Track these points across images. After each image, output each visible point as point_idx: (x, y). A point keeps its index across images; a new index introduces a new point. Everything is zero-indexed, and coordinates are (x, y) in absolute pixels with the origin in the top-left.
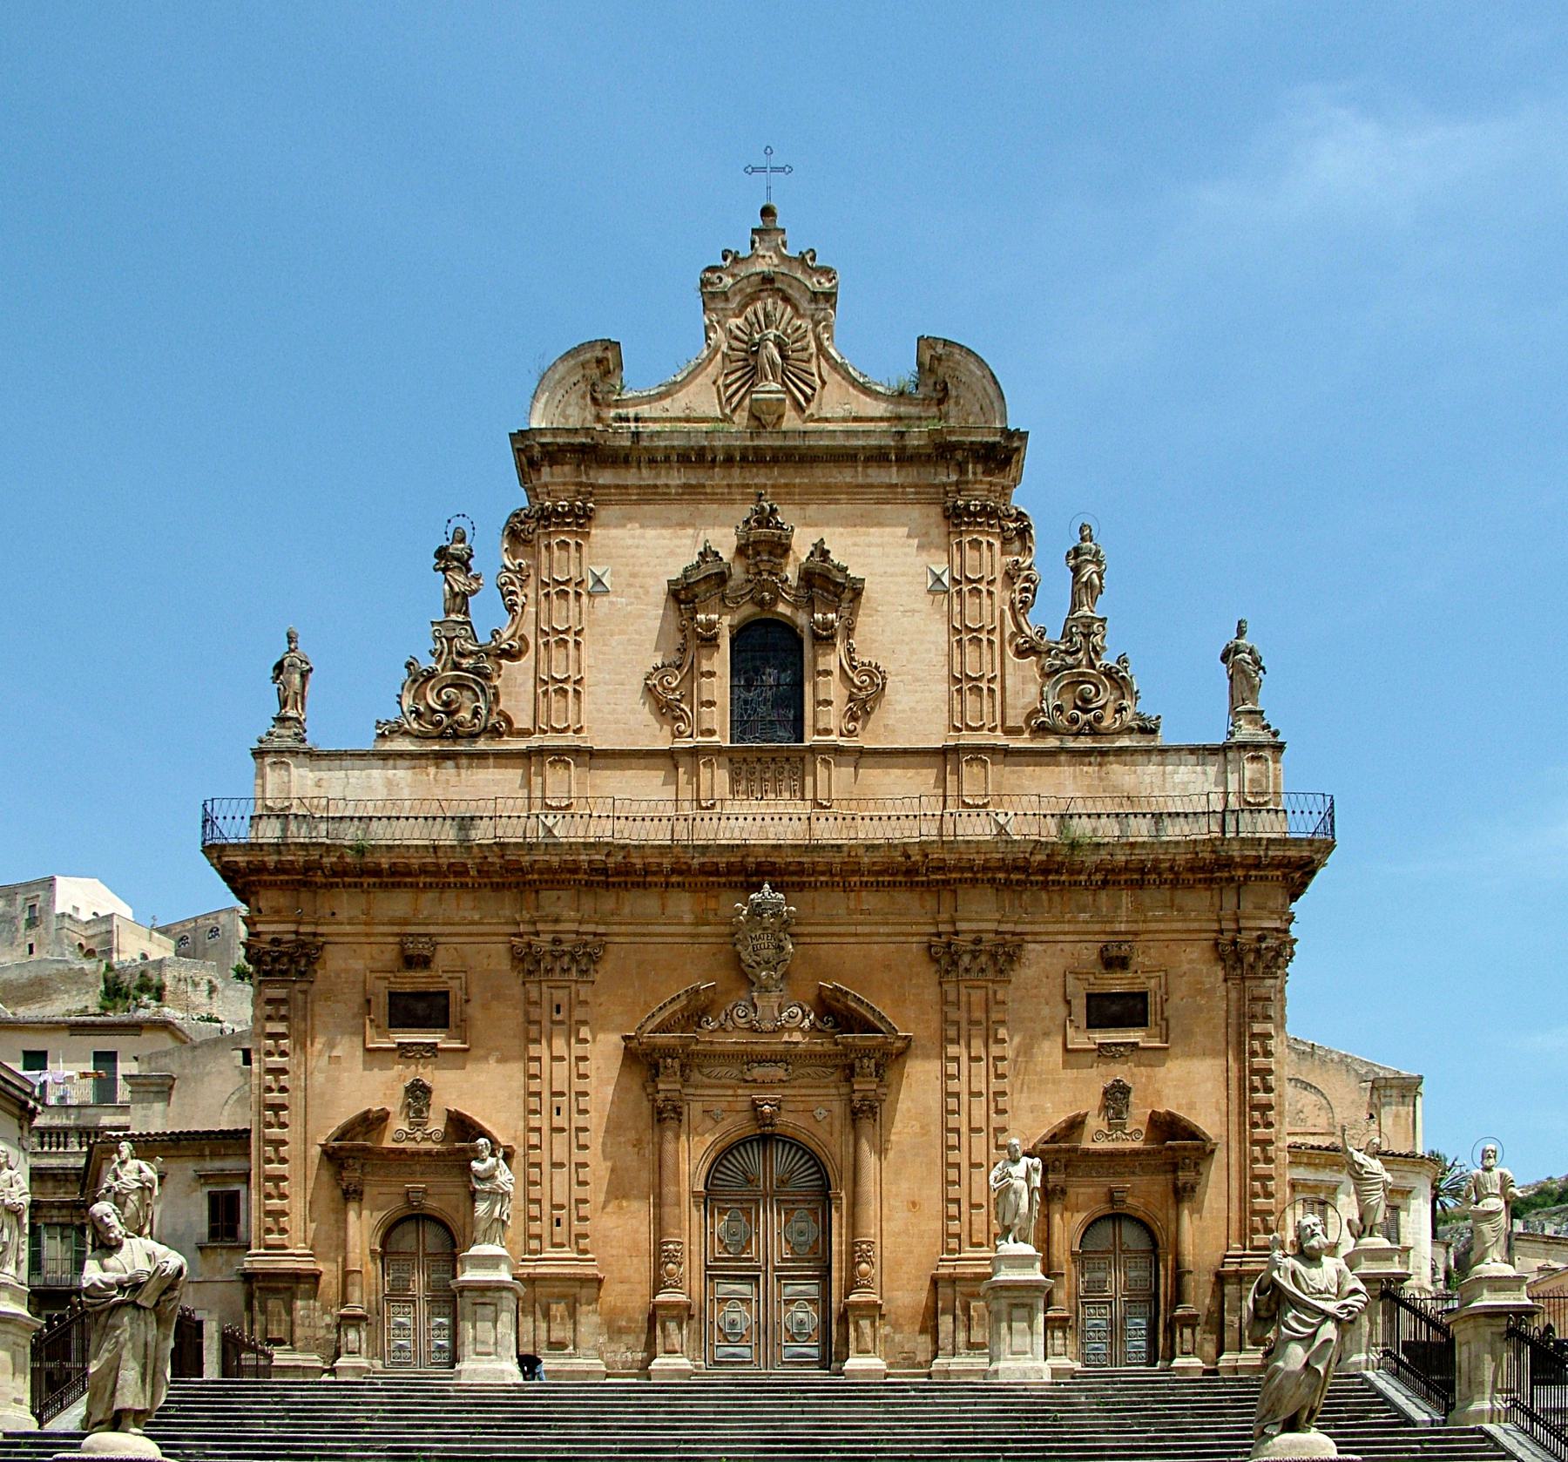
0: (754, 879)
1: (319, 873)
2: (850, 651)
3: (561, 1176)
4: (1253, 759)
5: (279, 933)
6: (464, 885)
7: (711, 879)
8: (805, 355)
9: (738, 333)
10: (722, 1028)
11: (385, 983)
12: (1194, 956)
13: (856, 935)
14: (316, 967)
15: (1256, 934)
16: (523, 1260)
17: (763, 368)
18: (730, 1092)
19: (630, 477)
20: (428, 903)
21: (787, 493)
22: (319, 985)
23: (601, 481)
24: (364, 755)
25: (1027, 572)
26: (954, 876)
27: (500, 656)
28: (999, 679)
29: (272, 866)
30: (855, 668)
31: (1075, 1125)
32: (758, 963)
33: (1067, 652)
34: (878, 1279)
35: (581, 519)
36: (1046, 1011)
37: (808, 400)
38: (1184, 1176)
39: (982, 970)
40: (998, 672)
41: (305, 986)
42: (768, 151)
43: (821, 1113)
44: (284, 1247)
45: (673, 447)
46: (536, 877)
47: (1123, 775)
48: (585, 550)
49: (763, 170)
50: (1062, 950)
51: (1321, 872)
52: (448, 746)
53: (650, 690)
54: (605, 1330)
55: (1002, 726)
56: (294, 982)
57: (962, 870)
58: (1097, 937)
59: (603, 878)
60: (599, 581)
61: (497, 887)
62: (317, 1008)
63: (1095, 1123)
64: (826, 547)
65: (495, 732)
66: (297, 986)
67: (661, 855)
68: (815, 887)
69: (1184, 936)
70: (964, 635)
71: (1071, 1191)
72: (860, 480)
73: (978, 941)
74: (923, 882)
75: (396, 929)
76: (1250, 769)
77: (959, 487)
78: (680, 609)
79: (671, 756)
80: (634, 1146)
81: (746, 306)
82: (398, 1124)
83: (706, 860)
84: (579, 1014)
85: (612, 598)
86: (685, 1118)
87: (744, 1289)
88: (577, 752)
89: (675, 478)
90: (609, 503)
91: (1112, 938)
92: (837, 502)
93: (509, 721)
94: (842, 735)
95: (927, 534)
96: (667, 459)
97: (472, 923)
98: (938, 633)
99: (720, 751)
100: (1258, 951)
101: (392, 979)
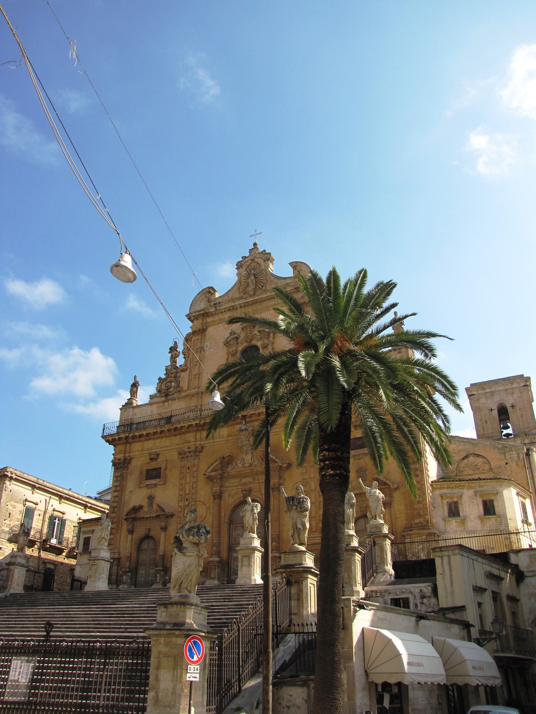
6: (166, 437)
19: (216, 318)
22: (129, 471)
42: (256, 231)
45: (226, 308)
49: (254, 235)
61: (175, 435)
82: (146, 509)
96: (225, 311)
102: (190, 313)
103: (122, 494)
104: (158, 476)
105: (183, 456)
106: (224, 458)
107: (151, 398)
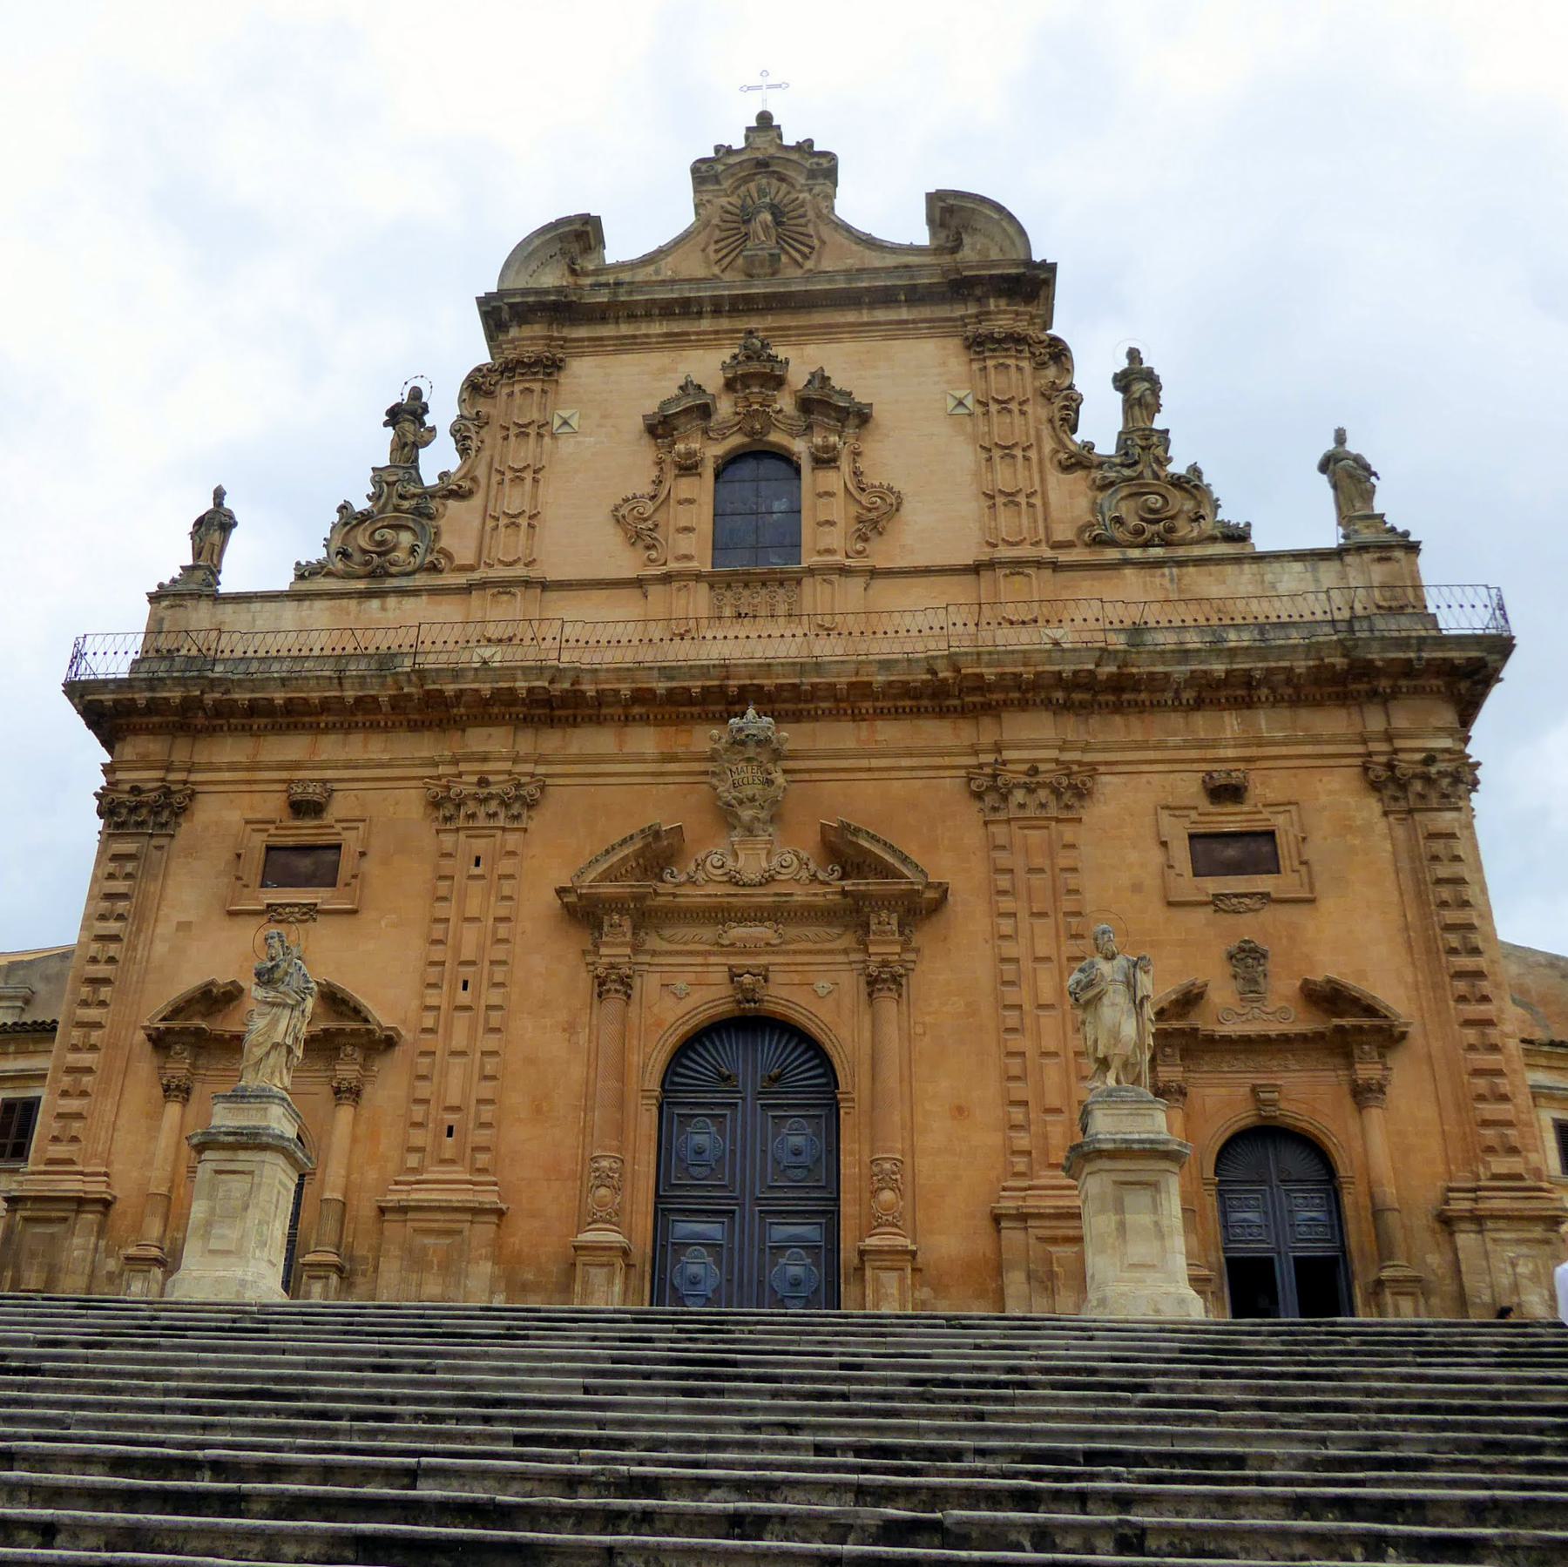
0: (737, 708)
1: (200, 714)
2: (857, 473)
3: (457, 1067)
4: (1380, 560)
5: (142, 781)
7: (682, 709)
8: (802, 221)
9: (730, 207)
10: (691, 881)
11: (264, 836)
12: (1336, 786)
13: (869, 770)
14: (181, 820)
15: (1419, 756)
16: (397, 1183)
17: (755, 232)
18: (700, 960)
20: (331, 748)
21: (784, 333)
22: (179, 842)
23: (574, 336)
24: (277, 596)
25: (1065, 392)
26: (995, 696)
27: (445, 497)
28: (1039, 495)
29: (142, 703)
30: (863, 490)
31: (1190, 1000)
32: (741, 802)
33: (1123, 465)
34: (909, 1217)
35: (550, 367)
36: (1133, 856)
37: (806, 257)
38: (1367, 1071)
39: (1043, 806)
40: (1037, 487)
41: (163, 841)
43: (823, 985)
44: (71, 1162)
45: (654, 301)
46: (462, 710)
47: (1206, 583)
48: (551, 396)
50: (1149, 783)
51: (1496, 692)
52: (374, 585)
53: (618, 521)
54: (503, 1285)
55: (1047, 542)
56: (151, 835)
57: (1006, 689)
58: (1195, 766)
59: (547, 711)
60: (565, 423)
62: (173, 865)
63: (1222, 993)
64: (826, 374)
65: (434, 568)
66: (155, 842)
67: (619, 680)
68: (816, 719)
69: (1319, 762)
70: (995, 451)
71: (1191, 1091)
72: (865, 319)
73: (1034, 771)
74: (955, 707)
75: (285, 775)
76: (1379, 573)
77: (980, 318)
78: (656, 445)
79: (639, 583)
80: (564, 1030)
81: (737, 188)
83: (674, 684)
84: (506, 866)
85: (580, 439)
86: (635, 994)
87: (712, 1229)
88: (527, 583)
89: (657, 328)
90: (582, 355)
91: (1216, 766)
92: (839, 341)
93: (449, 556)
94: (848, 556)
95: (944, 364)
97: (381, 765)
98: (965, 456)
99: (698, 577)
100: (1427, 780)
101: (273, 831)
102: (501, 294)
103: (139, 930)
104: (327, 877)
105: (448, 810)
106: (657, 834)
107: (300, 577)
